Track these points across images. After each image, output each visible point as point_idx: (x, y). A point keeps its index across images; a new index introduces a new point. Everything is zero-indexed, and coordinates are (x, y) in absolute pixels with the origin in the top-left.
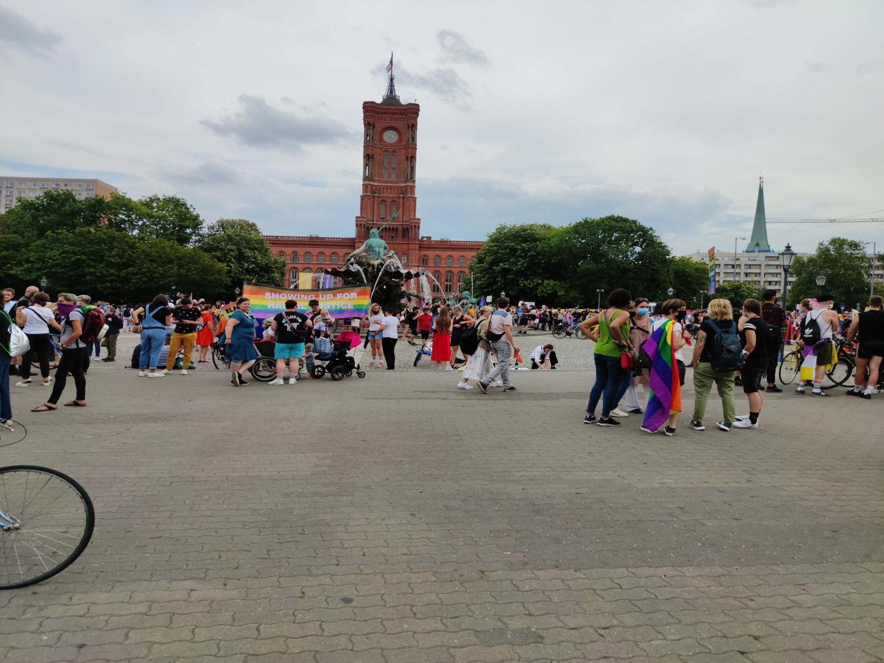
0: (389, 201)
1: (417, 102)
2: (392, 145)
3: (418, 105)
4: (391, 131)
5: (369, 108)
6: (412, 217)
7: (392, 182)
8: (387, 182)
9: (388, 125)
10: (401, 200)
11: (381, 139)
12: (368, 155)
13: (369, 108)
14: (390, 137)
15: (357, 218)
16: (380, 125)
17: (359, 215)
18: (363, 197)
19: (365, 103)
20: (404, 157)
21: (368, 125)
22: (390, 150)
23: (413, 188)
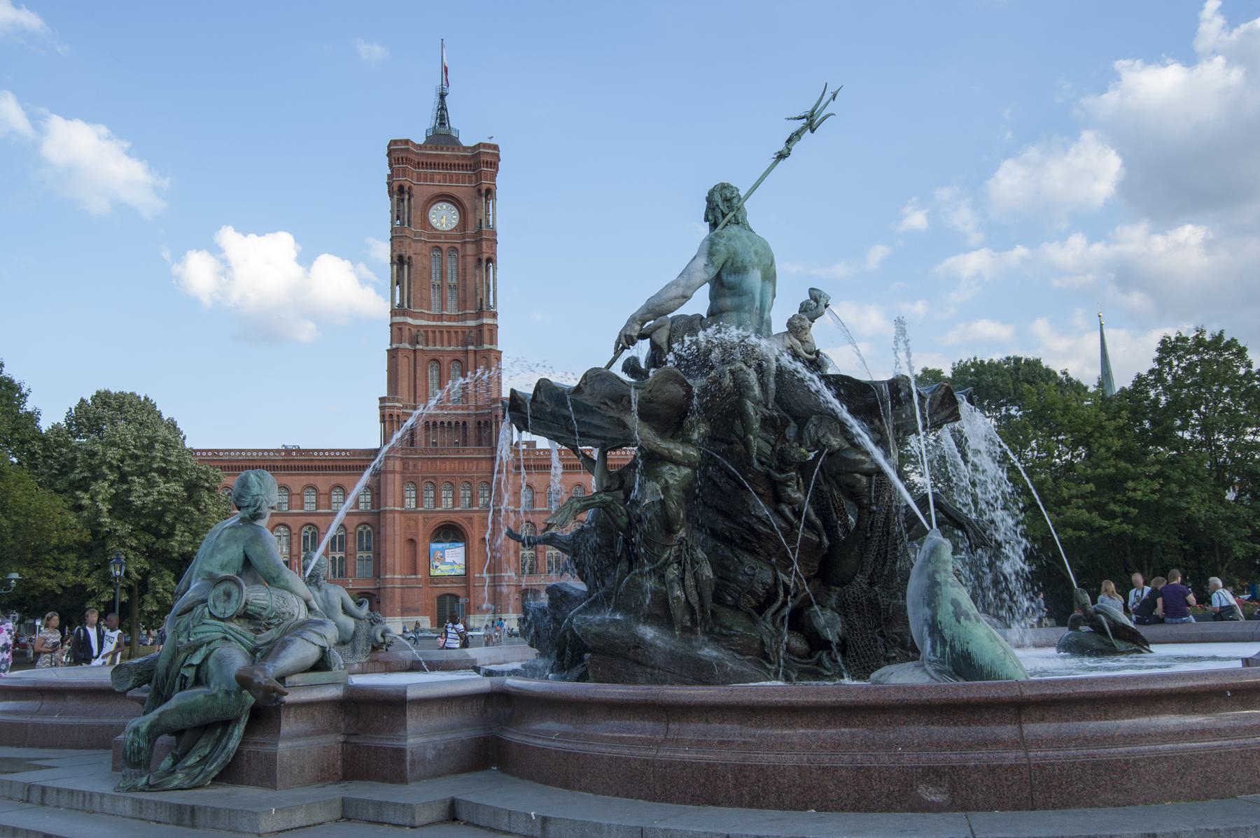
0: (446, 360)
1: (492, 142)
2: (447, 235)
3: (496, 147)
4: (445, 205)
5: (399, 153)
6: (494, 396)
7: (450, 318)
8: (440, 317)
9: (438, 190)
10: (471, 357)
11: (425, 222)
12: (401, 258)
13: (399, 153)
14: (444, 218)
15: (382, 400)
16: (421, 192)
17: (385, 395)
18: (392, 354)
19: (393, 142)
20: (471, 261)
21: (399, 192)
22: (445, 247)
23: (493, 329)
